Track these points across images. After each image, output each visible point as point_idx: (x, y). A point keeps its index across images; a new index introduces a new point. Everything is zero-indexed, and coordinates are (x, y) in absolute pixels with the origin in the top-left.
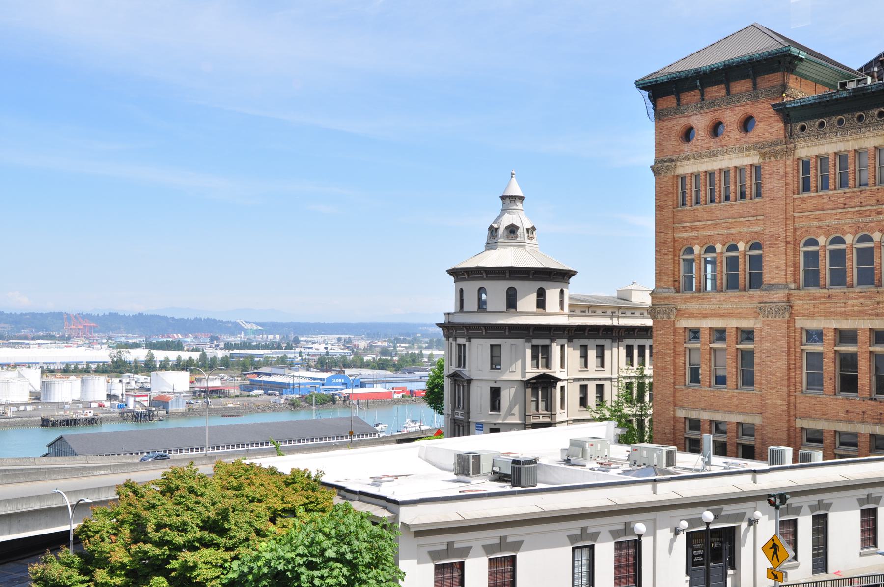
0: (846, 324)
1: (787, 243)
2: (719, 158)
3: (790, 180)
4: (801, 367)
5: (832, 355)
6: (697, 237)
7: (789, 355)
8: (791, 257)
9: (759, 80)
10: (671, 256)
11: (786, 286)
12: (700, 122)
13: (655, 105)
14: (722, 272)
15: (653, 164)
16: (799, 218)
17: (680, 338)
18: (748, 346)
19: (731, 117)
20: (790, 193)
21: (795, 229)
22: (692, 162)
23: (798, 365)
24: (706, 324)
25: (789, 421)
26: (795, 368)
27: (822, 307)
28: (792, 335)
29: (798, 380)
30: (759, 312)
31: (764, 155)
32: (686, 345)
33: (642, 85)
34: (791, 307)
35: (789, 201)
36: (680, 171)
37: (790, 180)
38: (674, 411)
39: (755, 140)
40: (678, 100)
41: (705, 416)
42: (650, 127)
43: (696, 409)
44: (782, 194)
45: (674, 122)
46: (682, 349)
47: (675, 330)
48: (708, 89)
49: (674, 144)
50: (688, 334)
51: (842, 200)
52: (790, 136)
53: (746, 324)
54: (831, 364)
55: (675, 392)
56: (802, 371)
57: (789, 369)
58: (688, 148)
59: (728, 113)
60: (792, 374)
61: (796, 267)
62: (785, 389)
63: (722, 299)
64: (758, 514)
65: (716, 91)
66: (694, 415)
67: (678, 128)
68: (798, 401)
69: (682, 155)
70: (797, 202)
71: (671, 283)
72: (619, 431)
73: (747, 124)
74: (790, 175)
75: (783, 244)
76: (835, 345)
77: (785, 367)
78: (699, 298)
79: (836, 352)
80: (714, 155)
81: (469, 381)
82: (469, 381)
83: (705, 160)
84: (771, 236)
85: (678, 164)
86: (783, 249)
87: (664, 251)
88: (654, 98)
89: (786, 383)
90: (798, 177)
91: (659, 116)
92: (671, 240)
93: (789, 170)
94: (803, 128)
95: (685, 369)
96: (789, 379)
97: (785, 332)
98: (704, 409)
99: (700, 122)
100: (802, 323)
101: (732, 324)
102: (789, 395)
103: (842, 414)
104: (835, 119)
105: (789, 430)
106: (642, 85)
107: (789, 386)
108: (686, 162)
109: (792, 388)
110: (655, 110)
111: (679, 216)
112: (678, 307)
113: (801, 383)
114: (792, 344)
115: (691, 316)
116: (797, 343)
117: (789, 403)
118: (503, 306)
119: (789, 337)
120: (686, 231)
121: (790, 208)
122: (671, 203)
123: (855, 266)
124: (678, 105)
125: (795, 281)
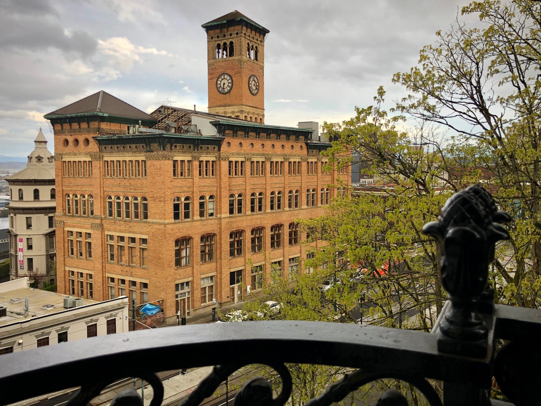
0: (121, 235)
1: (101, 197)
3: (101, 170)
4: (107, 251)
5: (116, 247)
6: (71, 191)
7: (102, 246)
8: (102, 204)
9: (90, 123)
10: (61, 198)
13: (54, 127)
14: (80, 207)
17: (66, 235)
18: (89, 240)
19: (81, 139)
20: (102, 176)
21: (104, 192)
24: (75, 230)
25: (103, 274)
27: (113, 227)
30: (93, 226)
31: (92, 158)
34: (103, 225)
35: (102, 179)
36: (64, 160)
37: (101, 170)
38: (65, 267)
39: (89, 151)
40: (62, 126)
41: (75, 270)
43: (72, 267)
44: (99, 176)
48: (72, 124)
49: (61, 146)
50: (70, 233)
52: (101, 151)
53: (89, 231)
54: (117, 251)
55: (64, 259)
56: (107, 253)
57: (102, 252)
59: (80, 136)
61: (105, 208)
64: (21, 341)
65: (75, 126)
66: (72, 269)
67: (63, 139)
69: (64, 153)
70: (105, 180)
72: (29, 282)
73: (87, 141)
76: (118, 243)
79: (118, 246)
80: (75, 155)
81: (16, 236)
82: (16, 236)
91: (56, 133)
93: (101, 166)
94: (105, 148)
95: (68, 249)
96: (102, 257)
98: (75, 267)
99: (71, 139)
100: (107, 233)
101: (84, 231)
102: (102, 263)
103: (120, 272)
104: (115, 146)
105: (103, 277)
113: (108, 258)
117: (103, 266)
118: (32, 198)
119: (102, 238)
121: (102, 183)
123: (124, 210)
124: (62, 128)
125: (104, 214)
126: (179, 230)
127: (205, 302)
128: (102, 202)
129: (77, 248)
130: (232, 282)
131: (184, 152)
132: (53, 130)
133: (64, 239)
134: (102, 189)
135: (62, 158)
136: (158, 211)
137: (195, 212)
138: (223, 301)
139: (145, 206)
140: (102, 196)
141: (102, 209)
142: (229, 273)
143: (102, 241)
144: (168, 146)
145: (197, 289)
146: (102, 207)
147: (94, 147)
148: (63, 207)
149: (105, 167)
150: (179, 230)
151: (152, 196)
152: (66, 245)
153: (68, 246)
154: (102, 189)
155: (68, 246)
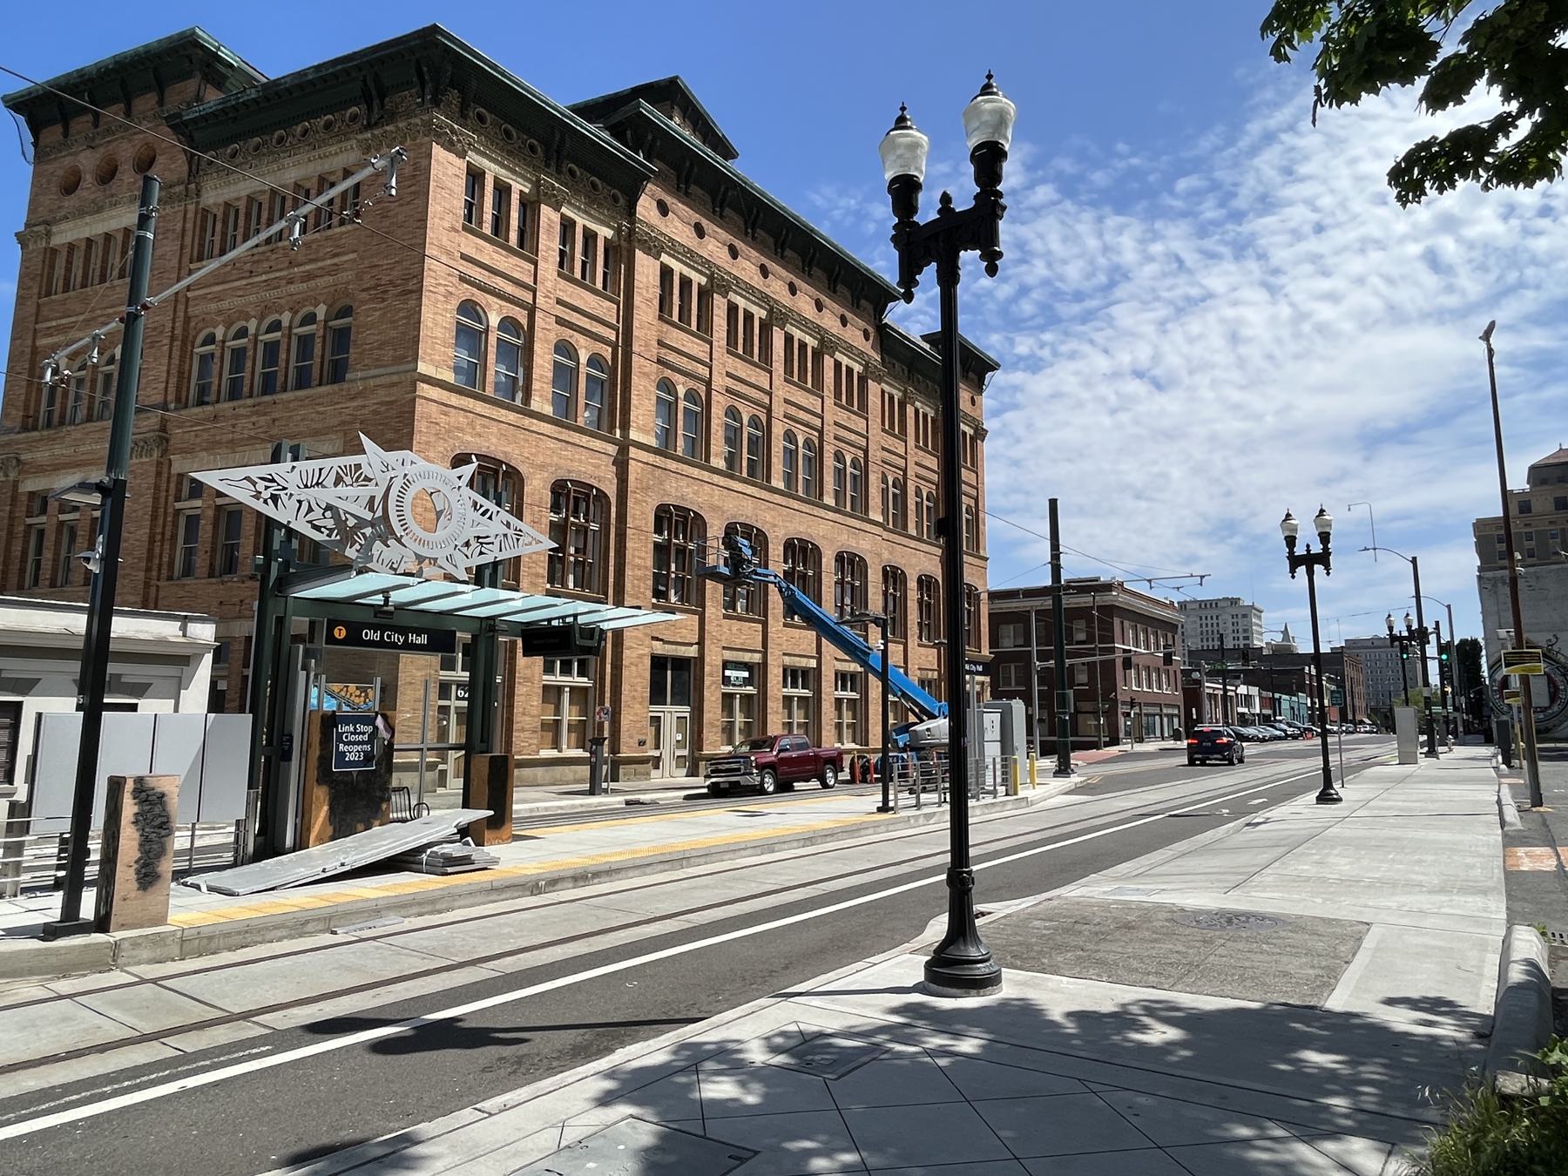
1: (173, 338)
2: (105, 215)
3: (188, 240)
4: (174, 537)
7: (154, 518)
8: (176, 361)
11: (164, 406)
12: (88, 161)
15: (22, 229)
16: (196, 298)
20: (186, 259)
21: (187, 320)
22: (71, 224)
23: (168, 535)
26: (162, 540)
27: (205, 436)
28: (164, 486)
29: (165, 559)
32: (29, 521)
33: (18, 104)
36: (57, 241)
37: (188, 240)
42: (25, 171)
44: (175, 262)
45: (56, 164)
46: (21, 528)
47: (14, 498)
51: (248, 267)
54: (210, 528)
57: (152, 541)
58: (70, 202)
59: (125, 145)
60: (157, 550)
62: (142, 575)
63: (79, 436)
67: (60, 172)
68: (162, 594)
71: (19, 419)
74: (189, 233)
75: (166, 341)
77: (145, 538)
78: (49, 438)
80: (100, 210)
83: (88, 219)
84: (155, 329)
85: (54, 229)
86: (166, 348)
87: (18, 369)
88: (36, 128)
89: (143, 564)
90: (202, 239)
91: (41, 155)
92: (28, 350)
93: (189, 225)
96: (150, 559)
97: (152, 480)
99: (88, 161)
102: (147, 585)
106: (18, 104)
107: (148, 570)
108: (64, 226)
109: (155, 573)
110: (35, 144)
111: (45, 312)
112: (23, 457)
114: (162, 501)
115: (40, 470)
116: (171, 499)
119: (157, 488)
120: (51, 335)
122: (36, 291)
126: (471, 424)
127: (556, 744)
128: (176, 353)
129: (57, 553)
130: (657, 696)
131: (510, 153)
132: (30, 151)
133: (11, 525)
134: (181, 307)
135: (49, 234)
136: (393, 333)
137: (536, 385)
138: (625, 753)
139: (342, 339)
140: (178, 331)
141: (173, 380)
142: (647, 651)
143: (156, 499)
144: (453, 96)
145: (527, 680)
146: (174, 371)
147: (171, 164)
148: (26, 408)
149: (203, 229)
150: (471, 424)
151: (373, 282)
152: (17, 548)
153: (24, 553)
154: (181, 307)
155: (24, 553)
